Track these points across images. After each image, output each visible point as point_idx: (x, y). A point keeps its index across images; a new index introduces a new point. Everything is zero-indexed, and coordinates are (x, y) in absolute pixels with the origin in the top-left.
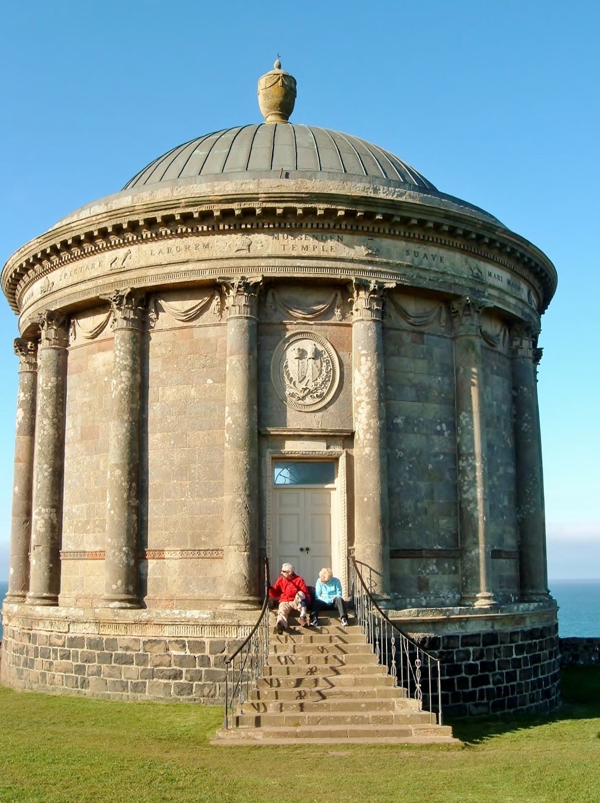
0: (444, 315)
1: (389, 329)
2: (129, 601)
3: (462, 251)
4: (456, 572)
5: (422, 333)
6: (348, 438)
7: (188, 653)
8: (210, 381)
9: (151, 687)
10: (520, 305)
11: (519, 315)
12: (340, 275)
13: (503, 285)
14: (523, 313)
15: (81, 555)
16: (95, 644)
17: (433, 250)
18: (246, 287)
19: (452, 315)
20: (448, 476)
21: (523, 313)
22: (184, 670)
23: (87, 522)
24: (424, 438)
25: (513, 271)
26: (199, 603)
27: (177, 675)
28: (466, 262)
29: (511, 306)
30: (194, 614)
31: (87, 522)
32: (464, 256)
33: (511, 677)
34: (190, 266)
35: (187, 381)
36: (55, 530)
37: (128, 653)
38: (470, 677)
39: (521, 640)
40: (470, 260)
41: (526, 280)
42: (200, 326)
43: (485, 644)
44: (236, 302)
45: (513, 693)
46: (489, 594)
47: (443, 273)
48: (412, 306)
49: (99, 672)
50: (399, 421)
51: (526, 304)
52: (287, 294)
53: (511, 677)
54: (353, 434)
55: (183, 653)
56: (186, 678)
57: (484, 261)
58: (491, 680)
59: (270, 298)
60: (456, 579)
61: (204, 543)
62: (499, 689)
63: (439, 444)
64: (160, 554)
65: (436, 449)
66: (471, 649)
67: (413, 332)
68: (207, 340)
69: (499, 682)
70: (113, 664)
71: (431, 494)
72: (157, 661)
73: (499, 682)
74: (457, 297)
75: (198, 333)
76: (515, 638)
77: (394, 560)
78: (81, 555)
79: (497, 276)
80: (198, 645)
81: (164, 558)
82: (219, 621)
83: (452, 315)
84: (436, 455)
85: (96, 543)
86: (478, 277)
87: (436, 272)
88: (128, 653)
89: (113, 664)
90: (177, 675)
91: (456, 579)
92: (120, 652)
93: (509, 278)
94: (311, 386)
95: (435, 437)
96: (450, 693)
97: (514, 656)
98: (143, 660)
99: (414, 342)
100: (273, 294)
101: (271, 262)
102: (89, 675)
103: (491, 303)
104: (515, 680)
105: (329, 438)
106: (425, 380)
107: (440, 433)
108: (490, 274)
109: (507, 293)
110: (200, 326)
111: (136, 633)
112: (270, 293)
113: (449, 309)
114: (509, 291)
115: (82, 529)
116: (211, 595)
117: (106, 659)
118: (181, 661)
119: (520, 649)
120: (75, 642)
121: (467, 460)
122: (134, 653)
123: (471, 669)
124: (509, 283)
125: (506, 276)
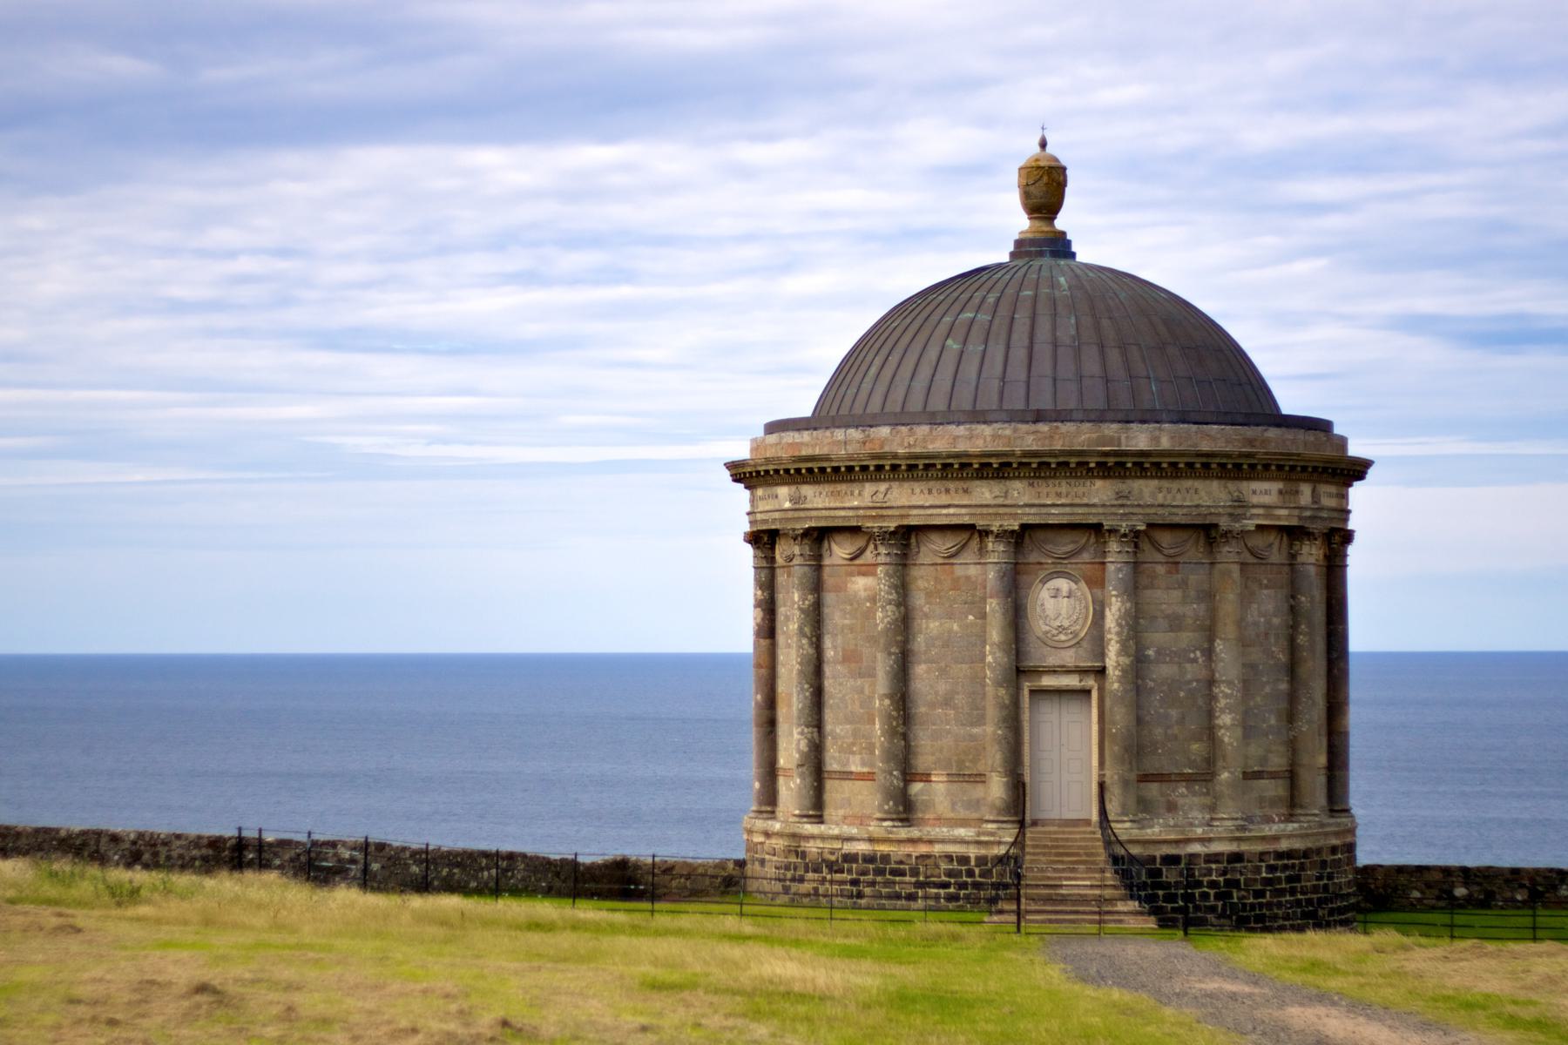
0: (1202, 542)
2: (901, 820)
4: (1208, 794)
6: (1101, 672)
16: (869, 859)
20: (1200, 702)
24: (1175, 668)
33: (1259, 894)
35: (950, 616)
38: (1212, 892)
43: (1229, 862)
48: (1165, 539)
50: (1151, 652)
52: (1040, 535)
60: (1208, 800)
62: (1244, 905)
63: (1194, 671)
64: (926, 778)
65: (1189, 676)
68: (968, 578)
71: (1181, 721)
73: (1244, 897)
74: (1216, 526)
75: (959, 571)
76: (1266, 857)
84: (1190, 682)
91: (1208, 800)
94: (1066, 623)
95: (1188, 666)
99: (1169, 572)
104: (1263, 896)
105: (1082, 672)
106: (1180, 610)
107: (1195, 660)
113: (1208, 536)
119: (1271, 869)
120: (850, 858)
123: (1213, 884)
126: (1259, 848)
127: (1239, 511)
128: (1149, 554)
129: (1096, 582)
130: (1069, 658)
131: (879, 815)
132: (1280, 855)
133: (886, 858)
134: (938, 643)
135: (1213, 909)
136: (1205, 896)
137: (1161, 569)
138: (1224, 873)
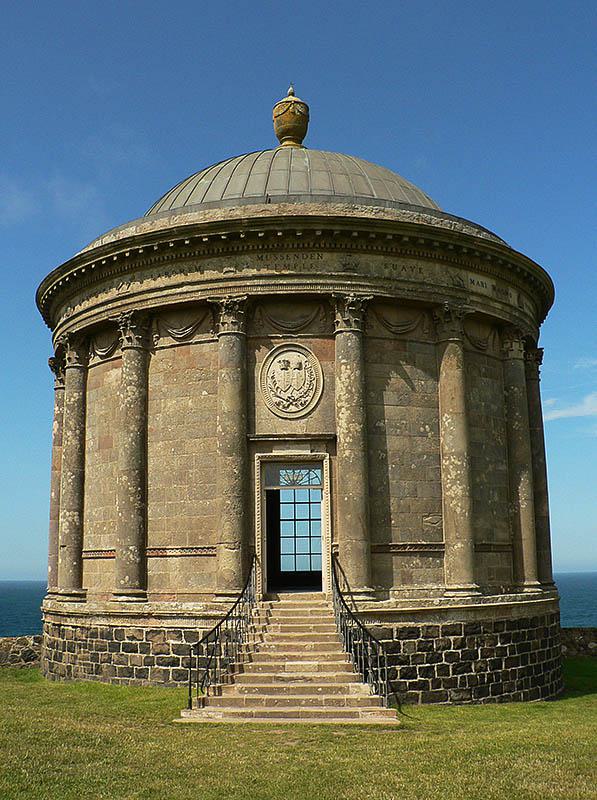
1: (371, 338)
3: (442, 262)
5: (405, 341)
6: (330, 442)
7: (184, 642)
8: (205, 393)
9: (152, 673)
10: (508, 309)
11: (507, 318)
12: (319, 290)
13: (487, 291)
14: (511, 315)
15: (99, 555)
16: (106, 635)
17: (413, 262)
18: (230, 308)
19: (436, 324)
21: (511, 315)
22: (181, 657)
23: (104, 525)
25: (497, 277)
26: (195, 597)
27: (175, 663)
28: (447, 272)
29: (497, 311)
30: (189, 606)
31: (104, 525)
32: (444, 267)
33: (496, 665)
34: (185, 289)
35: (185, 394)
36: (79, 530)
37: (134, 642)
39: (507, 630)
40: (450, 269)
41: (514, 286)
42: (196, 343)
44: (227, 322)
45: (498, 680)
46: (474, 586)
47: (423, 283)
48: (393, 317)
49: (109, 660)
51: (515, 309)
53: (496, 665)
54: (335, 437)
55: (180, 643)
56: (183, 665)
57: (466, 270)
58: (473, 667)
59: (257, 315)
61: (201, 542)
66: (452, 638)
67: (395, 339)
69: (481, 669)
70: (121, 652)
72: (157, 651)
73: (481, 669)
74: (440, 306)
77: (377, 555)
78: (99, 555)
79: (480, 284)
80: (191, 635)
81: (166, 556)
82: (210, 613)
83: (436, 324)
84: (420, 456)
85: (111, 543)
86: (460, 285)
87: (414, 283)
88: (134, 642)
89: (121, 652)
90: (175, 663)
92: (127, 641)
93: (494, 284)
96: (430, 680)
97: (499, 645)
98: (145, 649)
100: (260, 311)
101: (256, 282)
102: (102, 663)
103: (473, 309)
108: (473, 282)
109: (491, 299)
110: (196, 343)
111: (140, 623)
112: (257, 309)
114: (495, 297)
115: (98, 531)
116: (208, 590)
117: (115, 648)
118: (178, 650)
121: (449, 459)
122: (138, 642)
124: (494, 288)
125: (490, 282)
126: (494, 618)
127: (460, 295)
128: (377, 329)
129: (324, 355)
130: (299, 428)
131: (116, 591)
132: (512, 625)
133: (120, 633)
134: (174, 420)
135: (452, 683)
136: (443, 670)
137: (389, 346)
138: (462, 645)
